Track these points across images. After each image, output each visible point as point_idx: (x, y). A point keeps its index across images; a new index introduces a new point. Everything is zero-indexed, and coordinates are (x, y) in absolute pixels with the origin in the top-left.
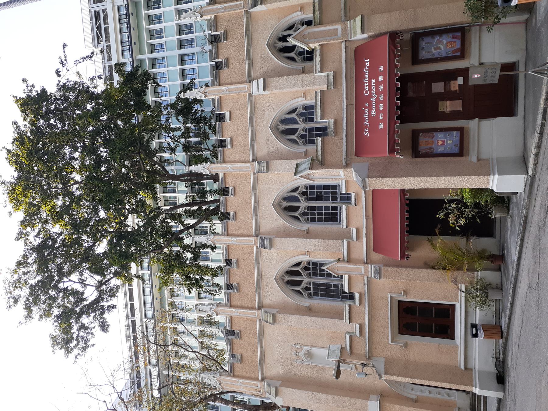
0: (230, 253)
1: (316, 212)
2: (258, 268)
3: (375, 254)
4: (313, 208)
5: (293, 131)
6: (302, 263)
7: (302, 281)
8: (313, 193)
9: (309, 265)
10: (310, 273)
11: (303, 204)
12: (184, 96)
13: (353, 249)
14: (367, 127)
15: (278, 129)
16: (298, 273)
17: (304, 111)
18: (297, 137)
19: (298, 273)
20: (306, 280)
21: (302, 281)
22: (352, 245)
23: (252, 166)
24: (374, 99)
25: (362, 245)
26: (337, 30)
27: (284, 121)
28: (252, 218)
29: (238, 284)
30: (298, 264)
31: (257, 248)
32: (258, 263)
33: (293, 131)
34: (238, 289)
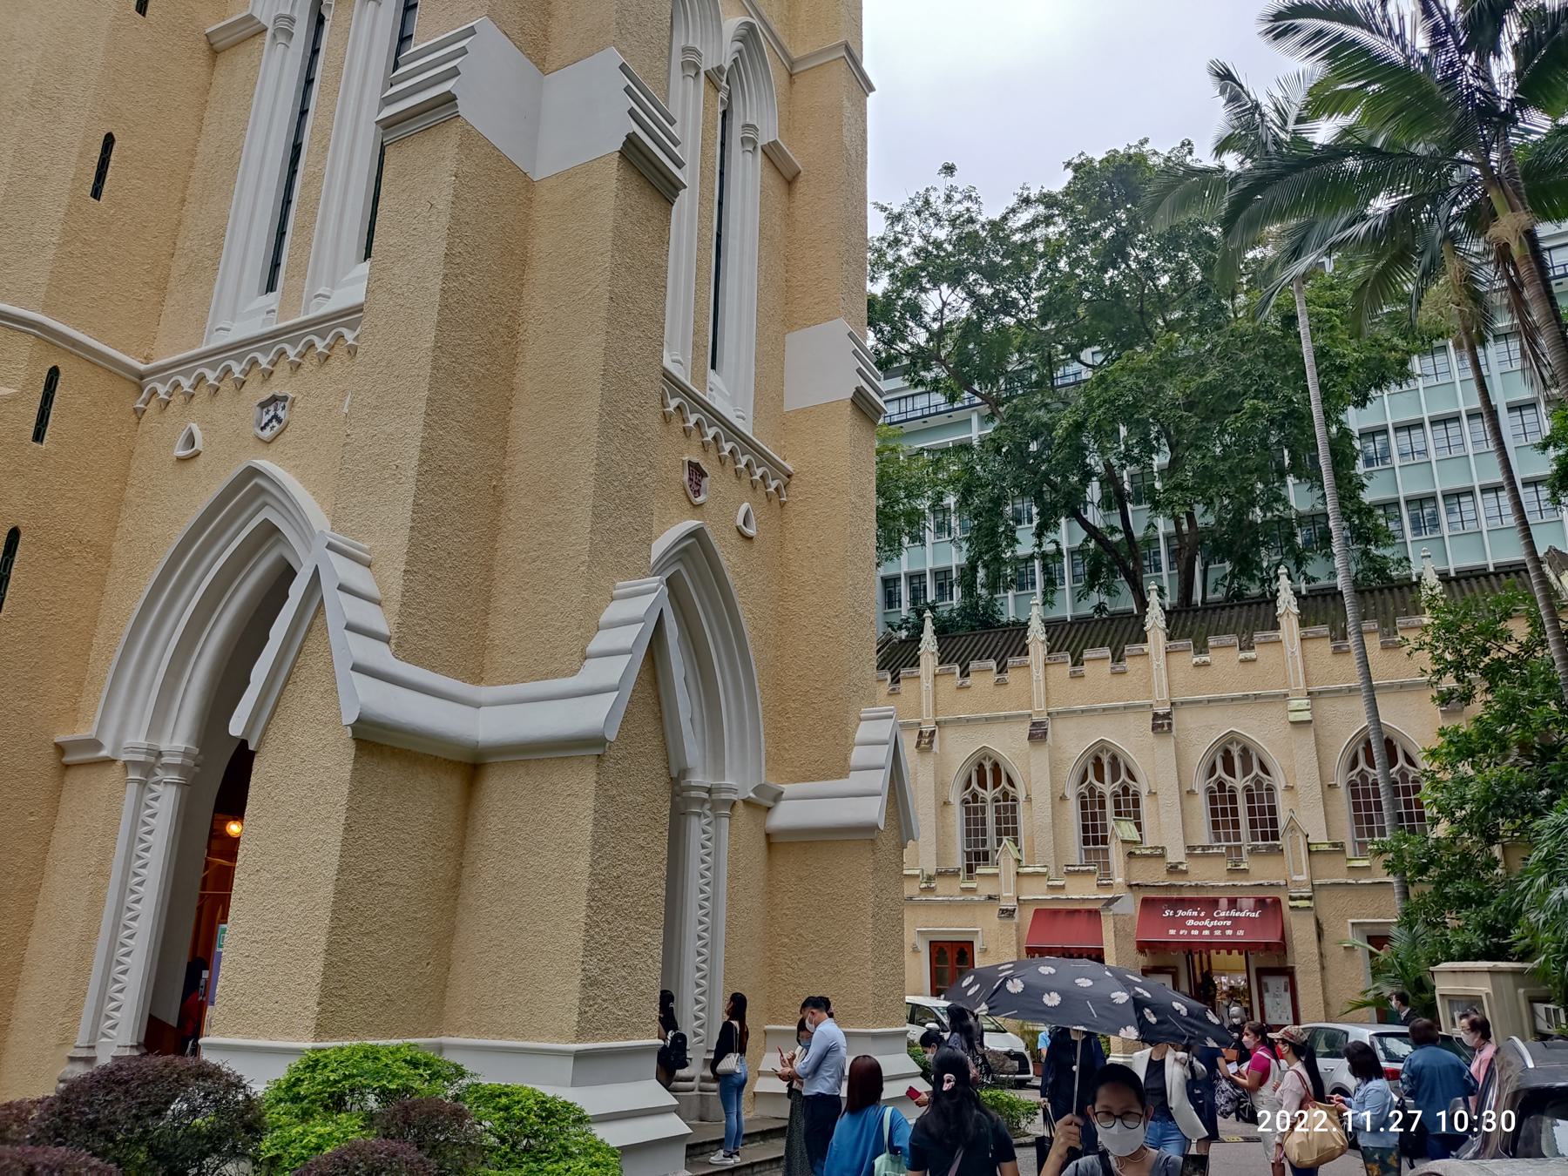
0: (1018, 670)
1: (1097, 810)
2: (998, 718)
3: (1032, 913)
4: (1102, 805)
5: (1229, 769)
6: (1013, 789)
7: (986, 789)
8: (1127, 805)
9: (1012, 800)
10: (999, 801)
11: (1107, 788)
12: (1282, 574)
13: (1035, 881)
14: (1175, 913)
15: (1231, 743)
16: (996, 783)
17: (1264, 787)
18: (1220, 777)
19: (996, 783)
20: (988, 794)
21: (986, 789)
22: (1040, 879)
23: (1164, 702)
24: (1207, 923)
25: (1044, 894)
26: (1302, 874)
27: (1245, 753)
28: (1077, 704)
29: (969, 687)
30: (1011, 782)
31: (1030, 715)
32: (1006, 717)
33: (1229, 769)
34: (961, 688)
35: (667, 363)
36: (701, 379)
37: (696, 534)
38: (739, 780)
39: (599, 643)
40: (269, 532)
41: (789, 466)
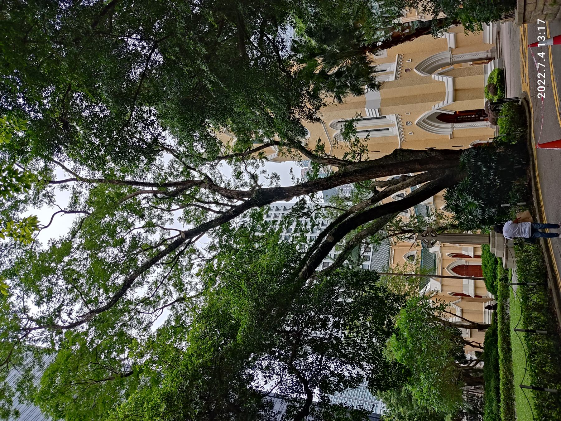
35: (392, 78)
36: (391, 73)
37: (416, 68)
38: (449, 55)
39: (441, 80)
40: (423, 121)
41: (397, 55)
